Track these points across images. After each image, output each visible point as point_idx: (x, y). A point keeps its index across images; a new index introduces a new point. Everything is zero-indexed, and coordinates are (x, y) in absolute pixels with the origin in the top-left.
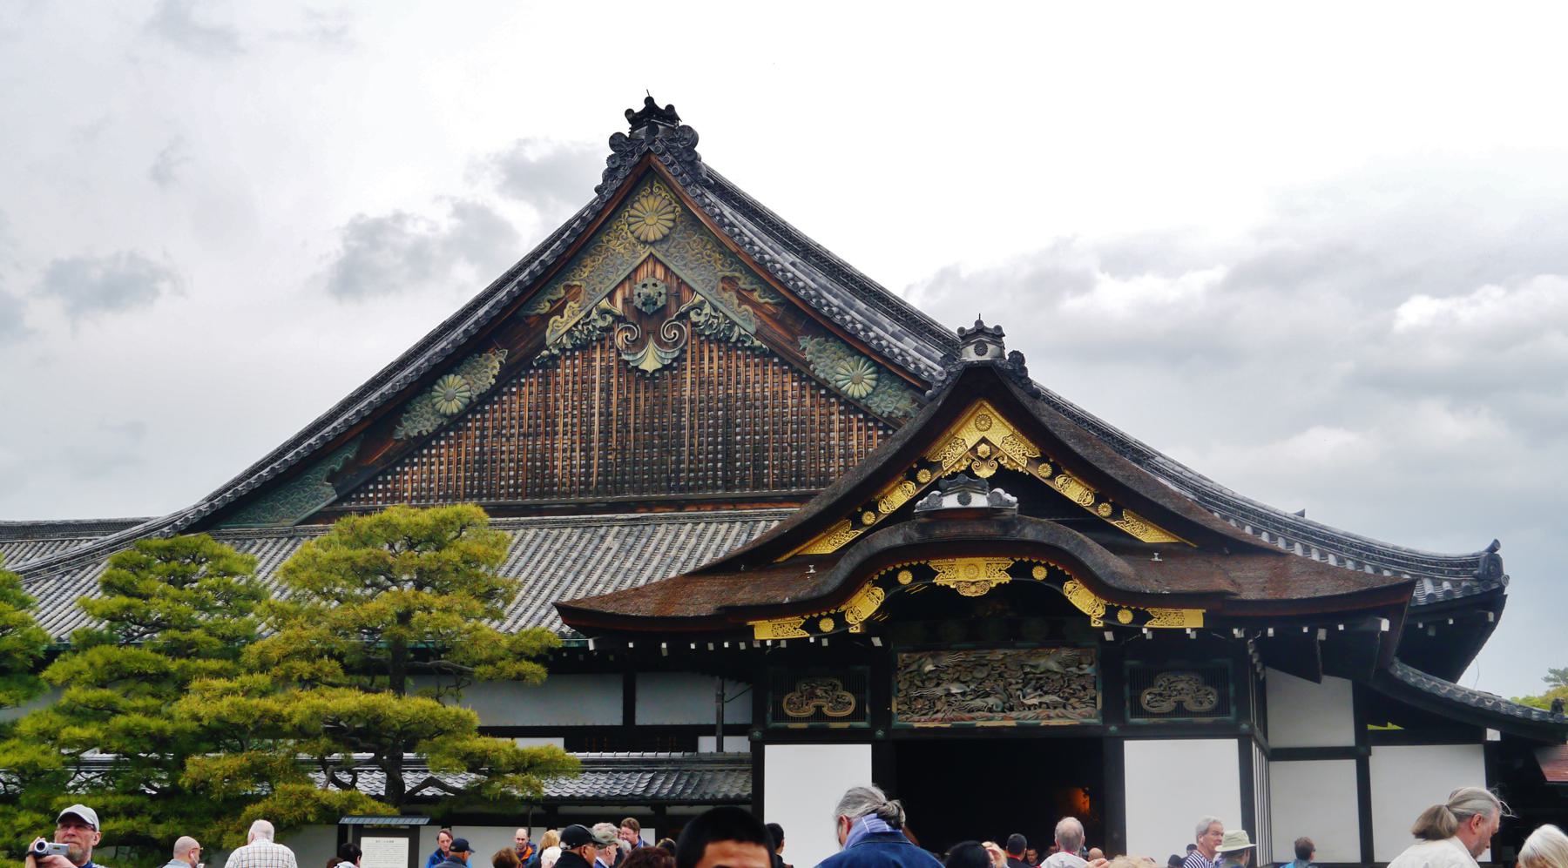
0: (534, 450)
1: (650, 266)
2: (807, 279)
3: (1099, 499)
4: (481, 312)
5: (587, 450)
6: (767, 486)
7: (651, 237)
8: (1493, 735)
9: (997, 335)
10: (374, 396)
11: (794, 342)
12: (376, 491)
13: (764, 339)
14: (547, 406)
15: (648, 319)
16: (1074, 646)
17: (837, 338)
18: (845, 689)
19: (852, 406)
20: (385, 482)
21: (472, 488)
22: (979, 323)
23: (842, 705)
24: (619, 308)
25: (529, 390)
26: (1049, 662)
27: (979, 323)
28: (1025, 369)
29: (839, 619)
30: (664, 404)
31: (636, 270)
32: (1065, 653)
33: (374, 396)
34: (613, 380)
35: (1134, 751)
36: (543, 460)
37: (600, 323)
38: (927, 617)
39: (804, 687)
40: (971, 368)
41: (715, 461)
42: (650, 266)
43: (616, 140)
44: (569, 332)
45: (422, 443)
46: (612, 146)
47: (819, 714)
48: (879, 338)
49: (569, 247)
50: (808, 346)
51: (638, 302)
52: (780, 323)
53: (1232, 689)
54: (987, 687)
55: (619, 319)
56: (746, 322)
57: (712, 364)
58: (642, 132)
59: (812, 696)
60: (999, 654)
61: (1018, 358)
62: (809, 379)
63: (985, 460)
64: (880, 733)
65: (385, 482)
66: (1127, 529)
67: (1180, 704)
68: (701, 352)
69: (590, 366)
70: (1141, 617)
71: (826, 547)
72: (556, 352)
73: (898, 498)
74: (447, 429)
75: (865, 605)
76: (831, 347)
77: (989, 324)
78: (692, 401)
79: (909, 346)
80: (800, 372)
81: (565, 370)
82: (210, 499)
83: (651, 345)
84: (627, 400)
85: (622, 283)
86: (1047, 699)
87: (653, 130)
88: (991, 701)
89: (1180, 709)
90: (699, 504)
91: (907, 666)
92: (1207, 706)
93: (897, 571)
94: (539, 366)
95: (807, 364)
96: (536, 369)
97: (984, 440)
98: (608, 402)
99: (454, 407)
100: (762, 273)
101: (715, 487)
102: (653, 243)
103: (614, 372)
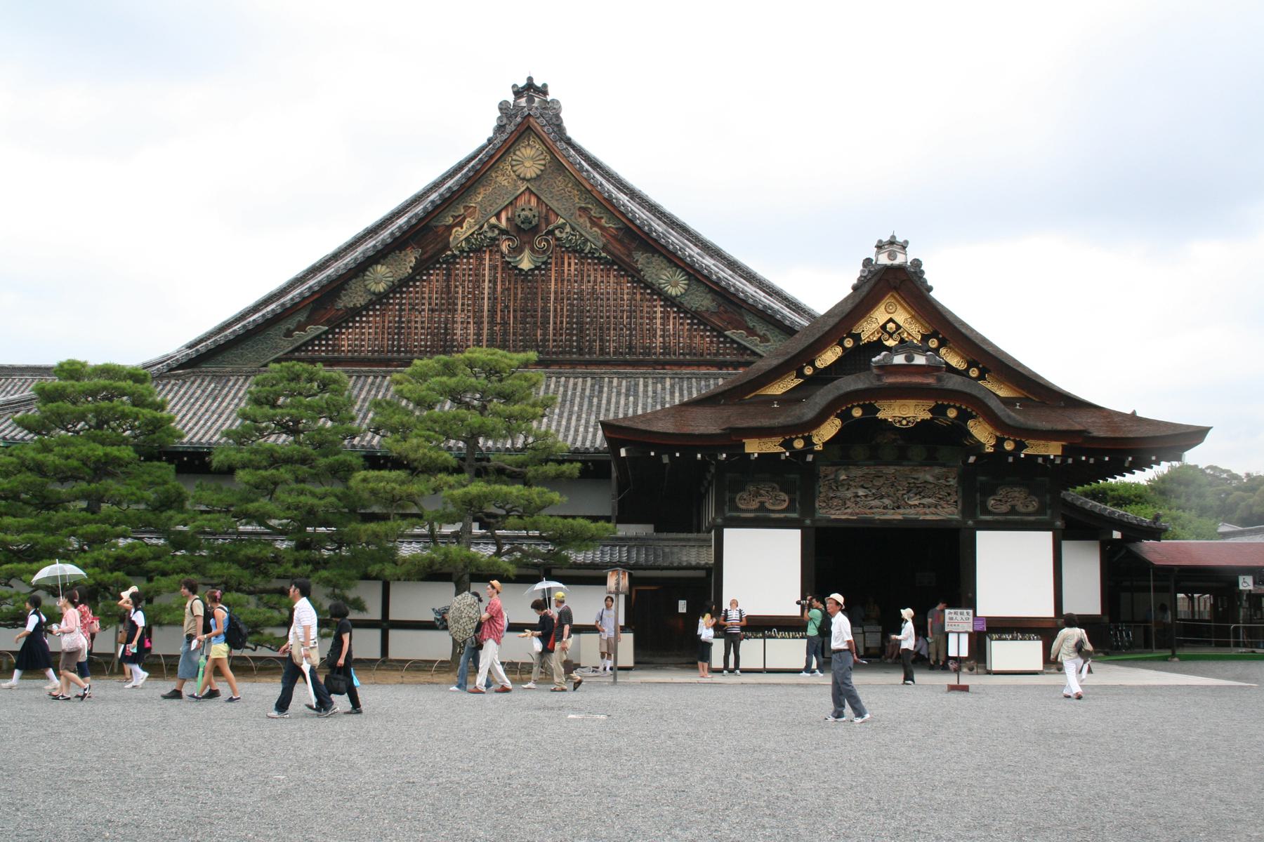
0: (439, 322)
1: (527, 197)
2: (642, 214)
3: (971, 364)
4: (402, 221)
5: (479, 324)
6: (608, 353)
7: (528, 176)
8: (1117, 535)
9: (904, 246)
10: (321, 277)
11: (630, 255)
12: (320, 345)
13: (609, 252)
14: (449, 292)
15: (524, 232)
16: (943, 465)
17: (661, 254)
18: (781, 490)
19: (669, 301)
20: (327, 339)
21: (393, 346)
22: (893, 237)
23: (779, 503)
24: (504, 223)
25: (435, 279)
26: (927, 475)
27: (893, 237)
28: (922, 272)
29: (809, 442)
30: (536, 293)
32: (937, 470)
33: (321, 277)
34: (499, 275)
35: (985, 540)
36: (446, 329)
37: (489, 234)
38: (865, 441)
39: (752, 488)
40: (887, 269)
41: (571, 335)
42: (527, 197)
43: (503, 107)
44: (467, 239)
45: (355, 312)
46: (501, 109)
47: (762, 507)
48: (690, 256)
49: (469, 179)
50: (641, 259)
51: (518, 221)
52: (620, 241)
53: (1048, 497)
54: (884, 491)
55: (502, 232)
56: (595, 238)
57: (571, 266)
58: (523, 102)
59: (758, 494)
60: (891, 470)
61: (917, 263)
62: (639, 281)
63: (891, 335)
64: (808, 522)
65: (327, 339)
66: (989, 386)
67: (1013, 507)
68: (563, 258)
69: (481, 264)
70: (1020, 446)
71: (778, 389)
72: (457, 253)
73: (829, 357)
74: (374, 304)
75: (829, 430)
76: (656, 260)
77: (900, 239)
78: (556, 293)
79: (708, 261)
80: (633, 276)
81: (463, 266)
82: (190, 346)
83: (527, 253)
84: (509, 289)
85: (506, 207)
86: (925, 501)
87: (530, 100)
88: (887, 501)
89: (1013, 511)
90: (560, 363)
91: (826, 476)
92: (1031, 509)
93: (853, 407)
94: (444, 262)
95: (639, 271)
96: (441, 264)
97: (891, 320)
98: (495, 289)
99: (381, 288)
100: (609, 206)
101: (571, 353)
102: (528, 180)
103: (499, 269)
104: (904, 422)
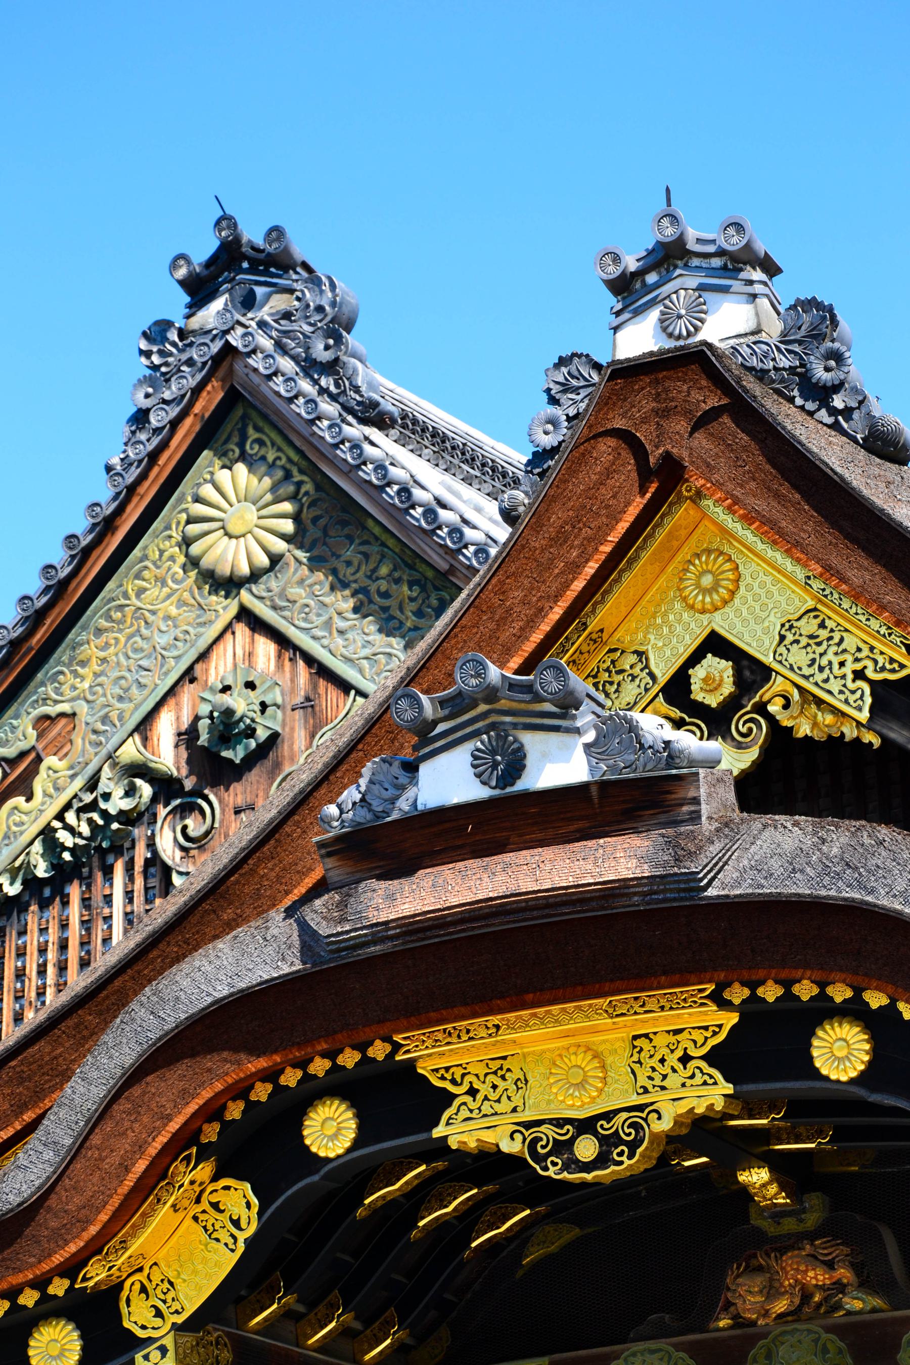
24: (167, 756)
31: (204, 656)
37: (118, 803)
85: (172, 692)
104: (586, 1148)
